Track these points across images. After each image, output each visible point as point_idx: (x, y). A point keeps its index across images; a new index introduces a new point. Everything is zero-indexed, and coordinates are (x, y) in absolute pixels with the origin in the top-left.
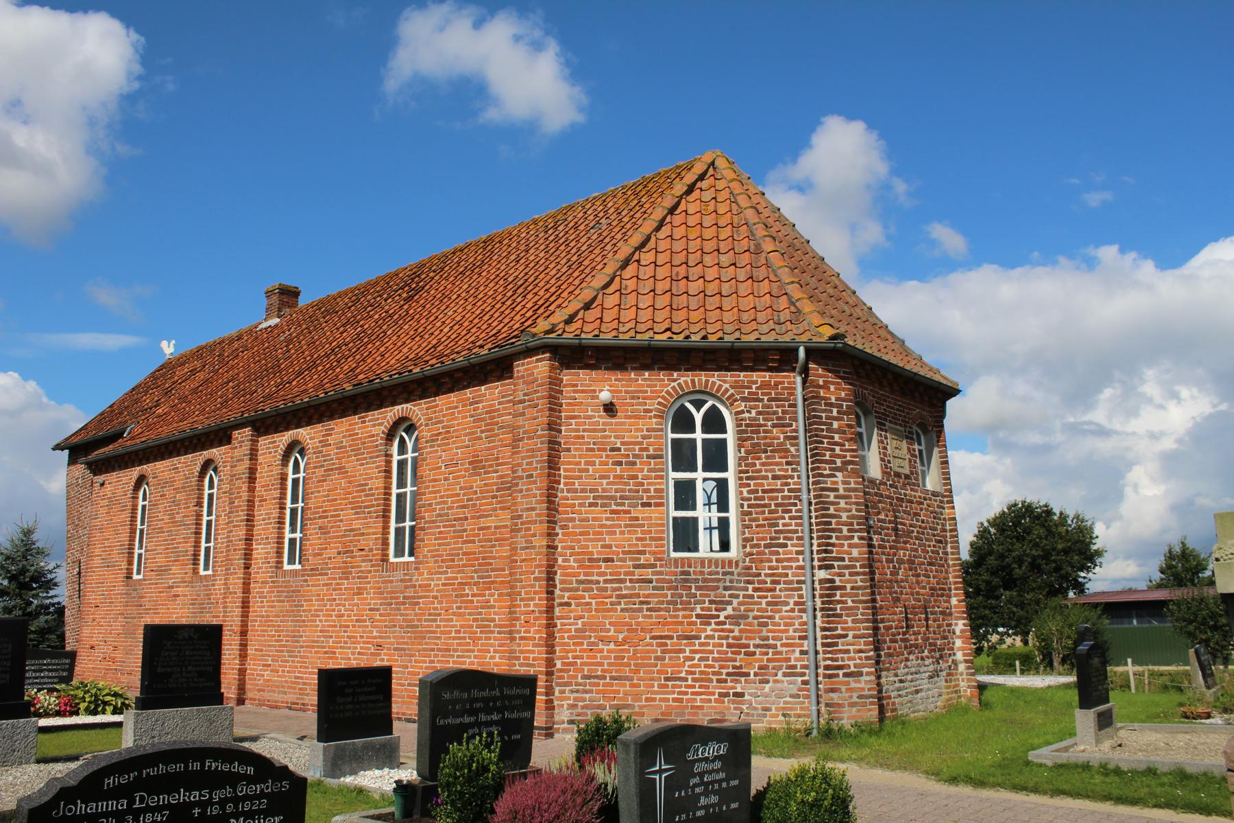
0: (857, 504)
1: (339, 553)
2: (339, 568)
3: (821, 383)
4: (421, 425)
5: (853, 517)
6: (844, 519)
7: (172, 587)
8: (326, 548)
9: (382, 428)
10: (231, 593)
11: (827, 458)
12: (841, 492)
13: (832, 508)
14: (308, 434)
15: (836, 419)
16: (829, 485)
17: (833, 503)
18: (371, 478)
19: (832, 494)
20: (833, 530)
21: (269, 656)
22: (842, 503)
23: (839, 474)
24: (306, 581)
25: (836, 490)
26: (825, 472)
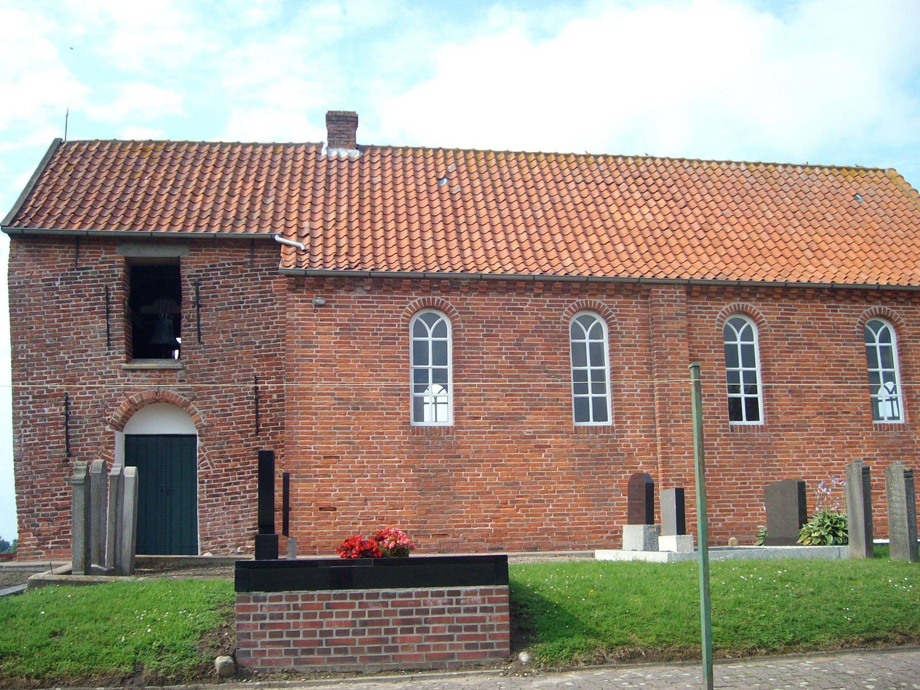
1: (821, 414)
2: (821, 426)
4: (902, 324)
7: (534, 437)
8: (801, 409)
9: (859, 319)
10: (673, 444)
14: (760, 309)
18: (852, 357)
21: (731, 502)
24: (779, 435)
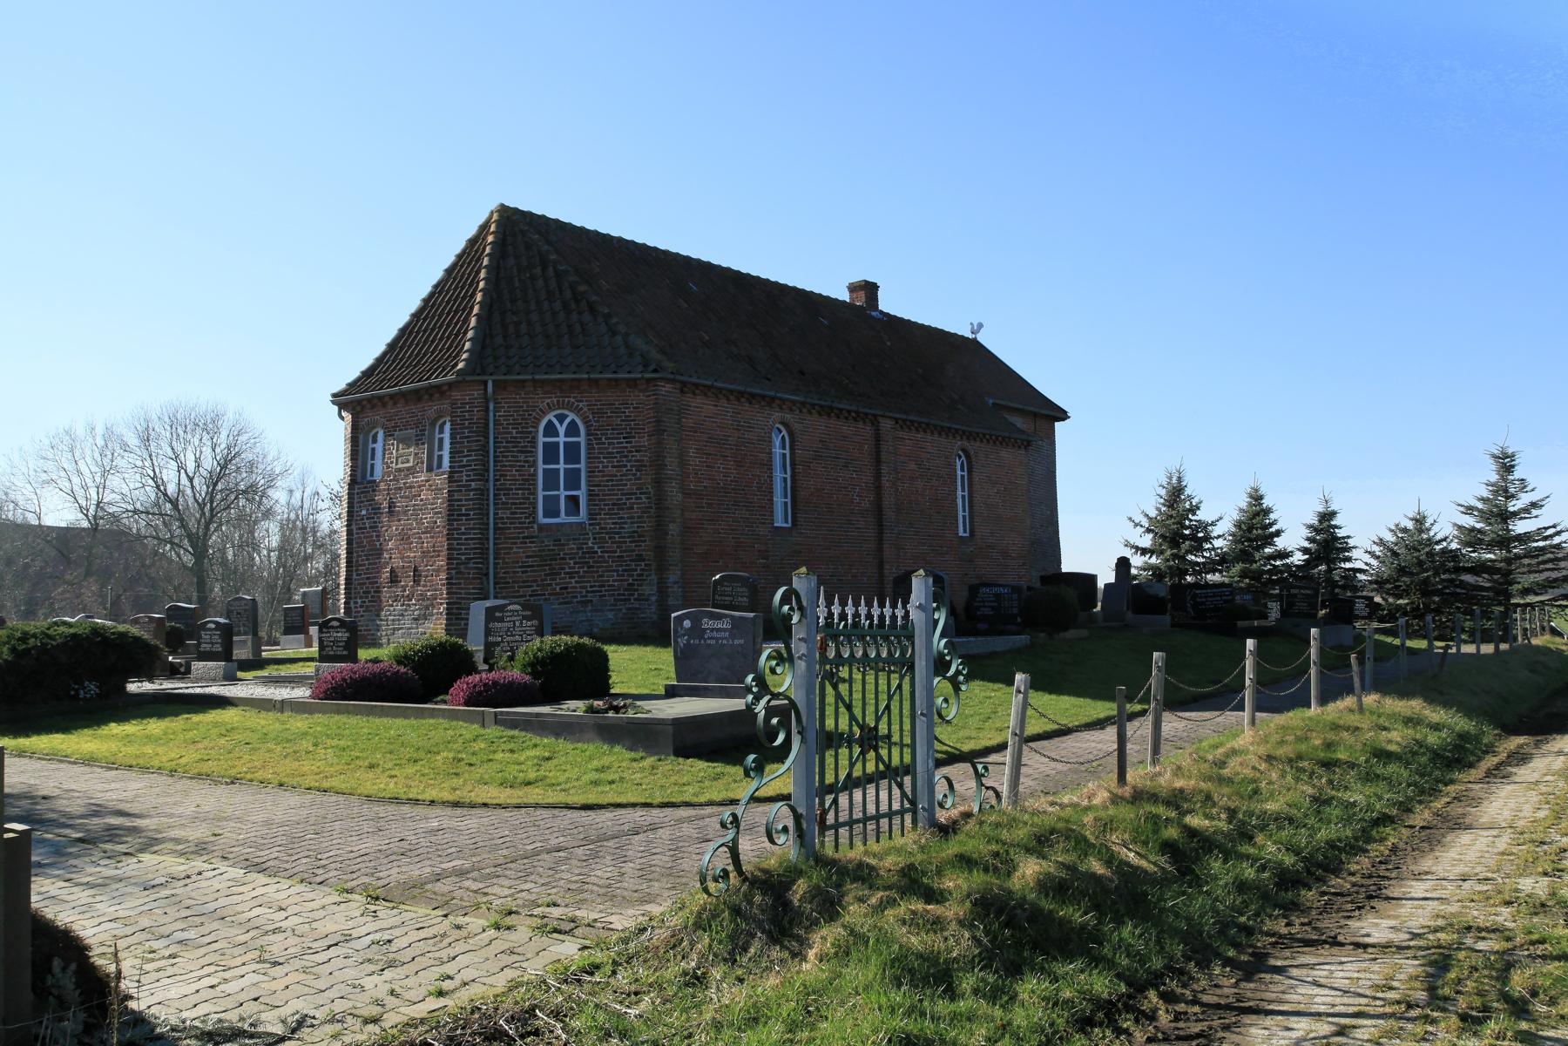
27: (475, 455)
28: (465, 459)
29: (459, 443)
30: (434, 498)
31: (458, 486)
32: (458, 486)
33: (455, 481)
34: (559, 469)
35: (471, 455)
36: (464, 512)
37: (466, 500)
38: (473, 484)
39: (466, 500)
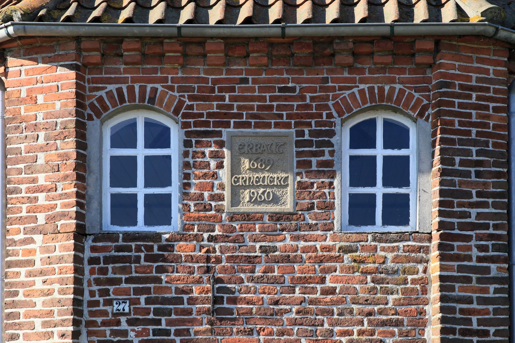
0: (61, 281)
3: (24, 95)
5: (53, 303)
6: (39, 307)
11: (24, 214)
12: (38, 266)
13: (21, 291)
15: (41, 149)
16: (20, 258)
17: (23, 285)
19: (23, 270)
20: (20, 326)
22: (39, 285)
23: (38, 238)
25: (31, 263)
26: (17, 238)
27: (495, 205)
28: (474, 212)
29: (460, 174)
30: (372, 291)
31: (461, 269)
32: (461, 269)
33: (457, 258)
34: (146, 186)
35: (485, 205)
36: (475, 326)
37: (482, 301)
38: (493, 266)
39: (482, 301)
